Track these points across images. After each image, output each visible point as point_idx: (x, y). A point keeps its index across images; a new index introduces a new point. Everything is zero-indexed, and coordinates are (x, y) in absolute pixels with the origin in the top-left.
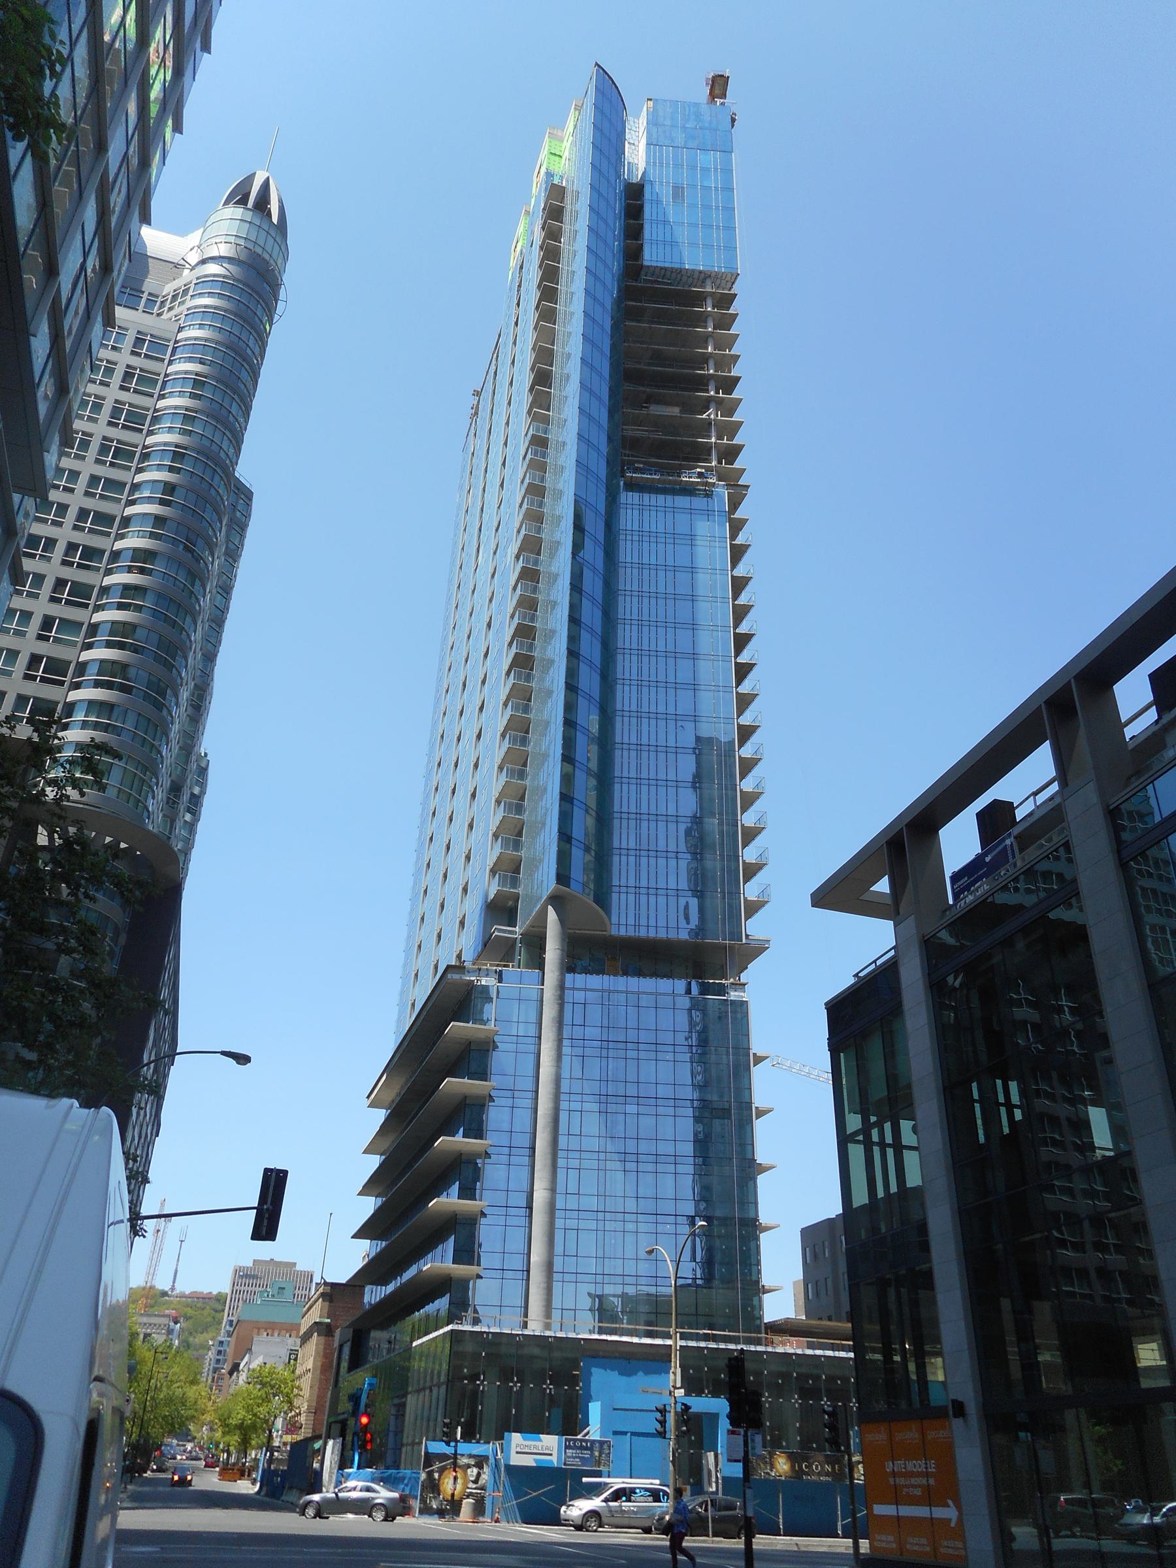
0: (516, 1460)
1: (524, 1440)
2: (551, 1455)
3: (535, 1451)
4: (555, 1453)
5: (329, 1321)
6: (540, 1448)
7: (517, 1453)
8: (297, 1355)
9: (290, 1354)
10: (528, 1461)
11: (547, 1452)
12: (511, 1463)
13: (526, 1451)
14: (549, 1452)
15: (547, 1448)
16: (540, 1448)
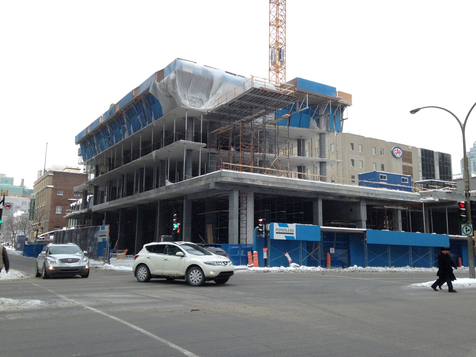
0: (277, 237)
1: (280, 226)
2: (293, 234)
3: (285, 232)
4: (295, 233)
5: (53, 186)
6: (288, 231)
7: (277, 233)
8: (35, 201)
9: (31, 201)
10: (282, 237)
11: (291, 232)
12: (274, 239)
13: (281, 232)
14: (293, 233)
15: (291, 230)
16: (288, 231)
